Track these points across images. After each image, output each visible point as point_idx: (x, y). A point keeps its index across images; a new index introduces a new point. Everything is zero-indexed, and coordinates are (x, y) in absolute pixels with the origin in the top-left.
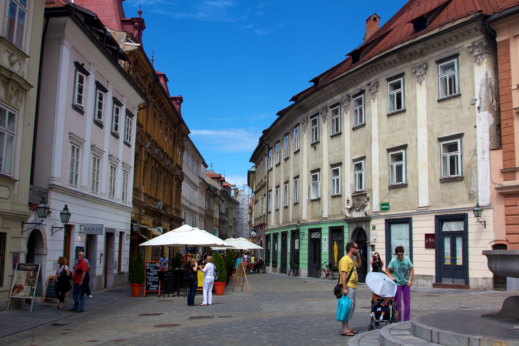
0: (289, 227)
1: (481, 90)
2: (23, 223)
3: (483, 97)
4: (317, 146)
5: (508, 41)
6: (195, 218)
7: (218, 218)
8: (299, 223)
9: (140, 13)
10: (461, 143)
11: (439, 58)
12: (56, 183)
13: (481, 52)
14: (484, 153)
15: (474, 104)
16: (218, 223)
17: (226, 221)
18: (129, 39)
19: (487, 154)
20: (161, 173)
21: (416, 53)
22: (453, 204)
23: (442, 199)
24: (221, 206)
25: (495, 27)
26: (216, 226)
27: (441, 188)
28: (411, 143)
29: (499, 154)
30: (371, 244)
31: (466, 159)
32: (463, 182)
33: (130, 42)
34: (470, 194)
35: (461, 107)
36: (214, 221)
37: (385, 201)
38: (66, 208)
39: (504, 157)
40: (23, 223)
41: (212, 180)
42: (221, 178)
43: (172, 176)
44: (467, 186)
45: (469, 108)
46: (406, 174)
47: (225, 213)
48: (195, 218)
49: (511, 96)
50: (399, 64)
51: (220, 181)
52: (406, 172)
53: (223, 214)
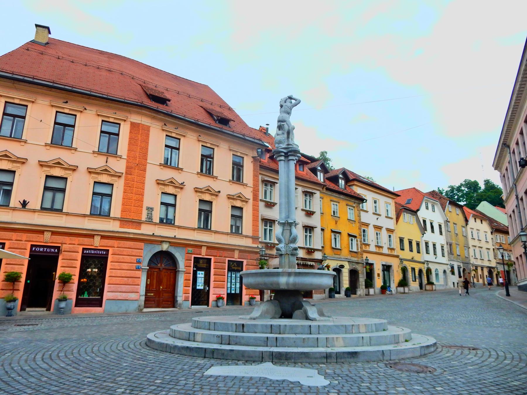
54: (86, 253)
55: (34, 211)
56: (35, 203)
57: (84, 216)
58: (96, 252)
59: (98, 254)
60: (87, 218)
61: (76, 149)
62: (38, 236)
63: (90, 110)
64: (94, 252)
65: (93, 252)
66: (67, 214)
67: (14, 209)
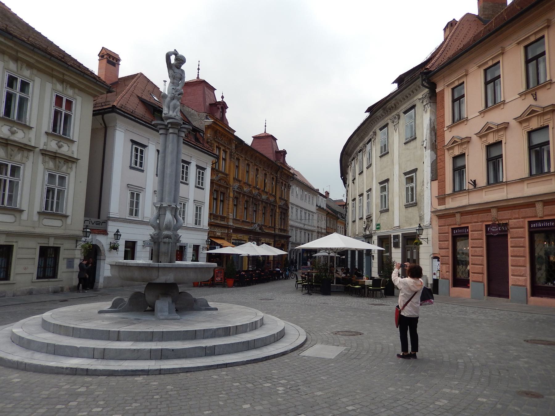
1: (427, 133)
2: (77, 241)
3: (428, 139)
4: (355, 181)
5: (443, 90)
9: (223, 97)
10: (416, 177)
11: (404, 110)
12: (111, 216)
13: (427, 102)
14: (428, 183)
15: (423, 145)
18: (208, 117)
19: (429, 184)
20: (259, 205)
21: (393, 107)
22: (411, 225)
23: (406, 220)
25: (435, 80)
27: (405, 212)
28: (391, 178)
29: (436, 183)
30: (373, 255)
31: (418, 188)
32: (416, 207)
33: (209, 119)
34: (420, 217)
35: (416, 148)
37: (378, 222)
38: (118, 231)
39: (438, 186)
40: (77, 241)
43: (275, 206)
44: (419, 210)
45: (421, 148)
46: (388, 201)
49: (444, 136)
50: (385, 117)
52: (388, 200)
54: (533, 228)
55: (482, 188)
56: (482, 181)
57: (522, 180)
58: (550, 224)
59: (546, 227)
60: (526, 183)
61: (504, 103)
62: (488, 215)
63: (510, 44)
64: (541, 225)
65: (540, 225)
66: (507, 183)
67: (469, 191)
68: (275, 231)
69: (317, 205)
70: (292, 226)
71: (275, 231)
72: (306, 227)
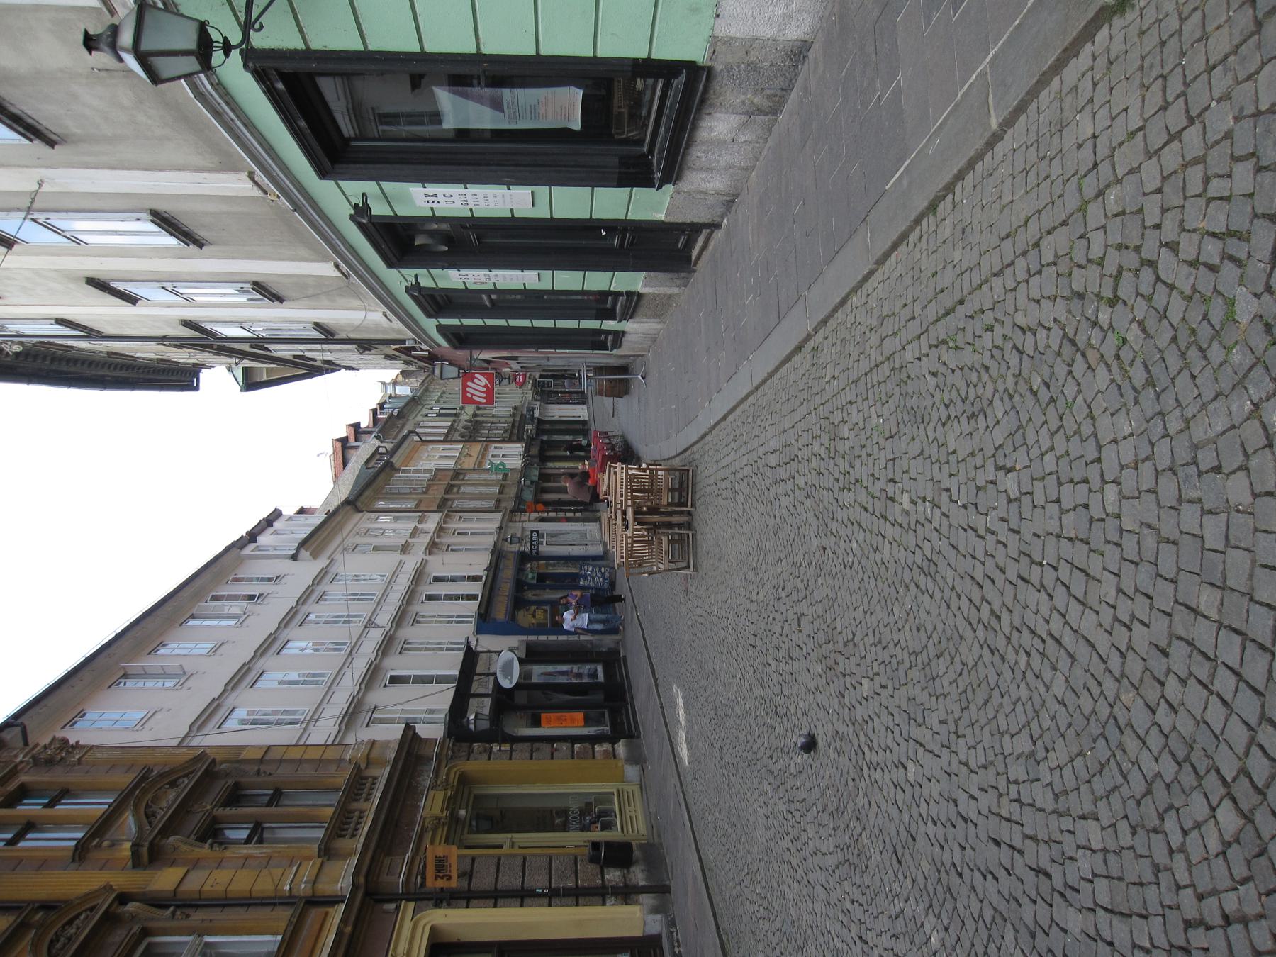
0: (305, 204)
6: (437, 579)
7: (460, 446)
8: (115, 30)
16: (476, 449)
17: (475, 415)
24: (426, 434)
26: (483, 456)
36: (468, 463)
41: (350, 466)
42: (343, 442)
47: (451, 419)
48: (437, 579)
51: (356, 440)
53: (451, 428)
68: (332, 901)
69: (294, 557)
70: (350, 717)
71: (332, 901)
72: (384, 618)
